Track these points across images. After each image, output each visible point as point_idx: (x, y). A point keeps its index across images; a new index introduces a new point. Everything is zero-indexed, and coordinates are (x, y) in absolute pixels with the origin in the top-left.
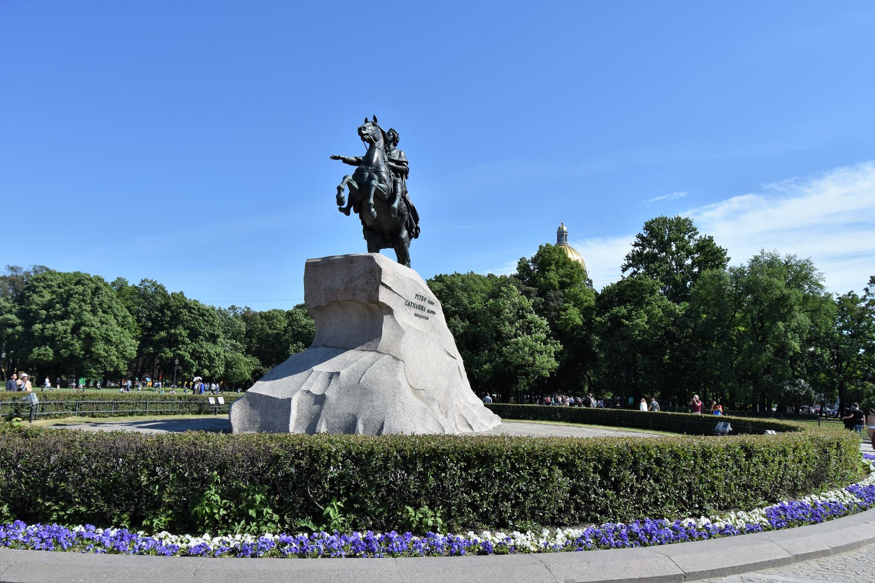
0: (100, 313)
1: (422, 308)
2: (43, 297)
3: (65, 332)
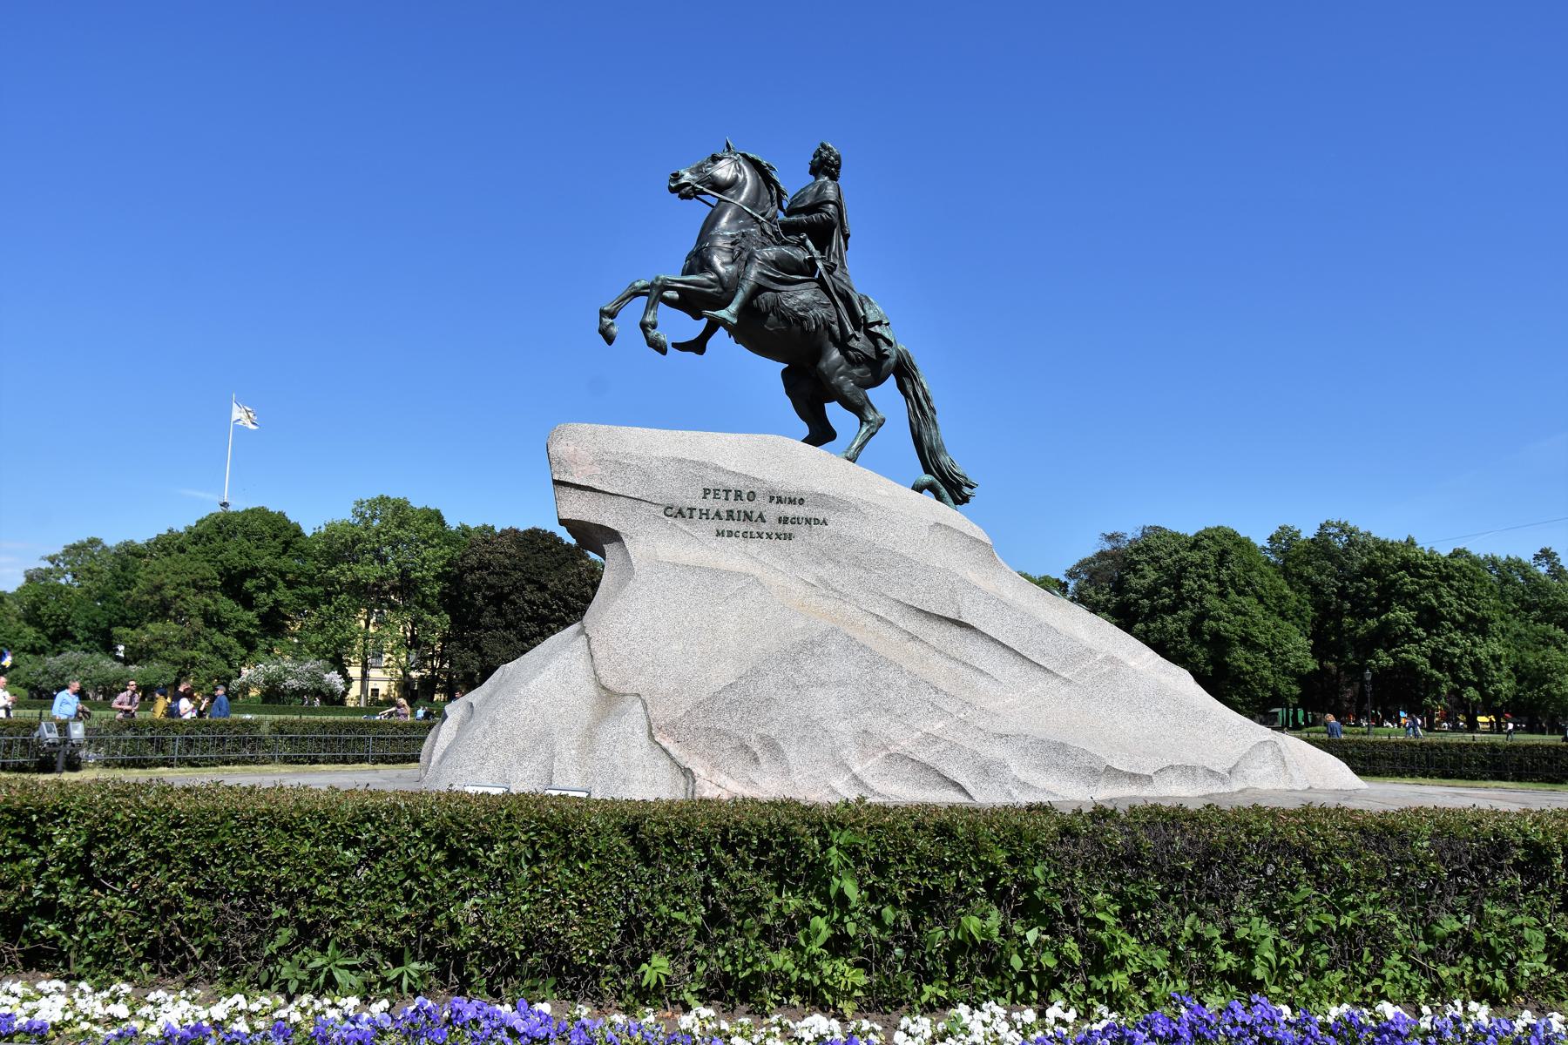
0: (1233, 595)
1: (748, 517)
2: (1144, 577)
3: (1180, 633)
